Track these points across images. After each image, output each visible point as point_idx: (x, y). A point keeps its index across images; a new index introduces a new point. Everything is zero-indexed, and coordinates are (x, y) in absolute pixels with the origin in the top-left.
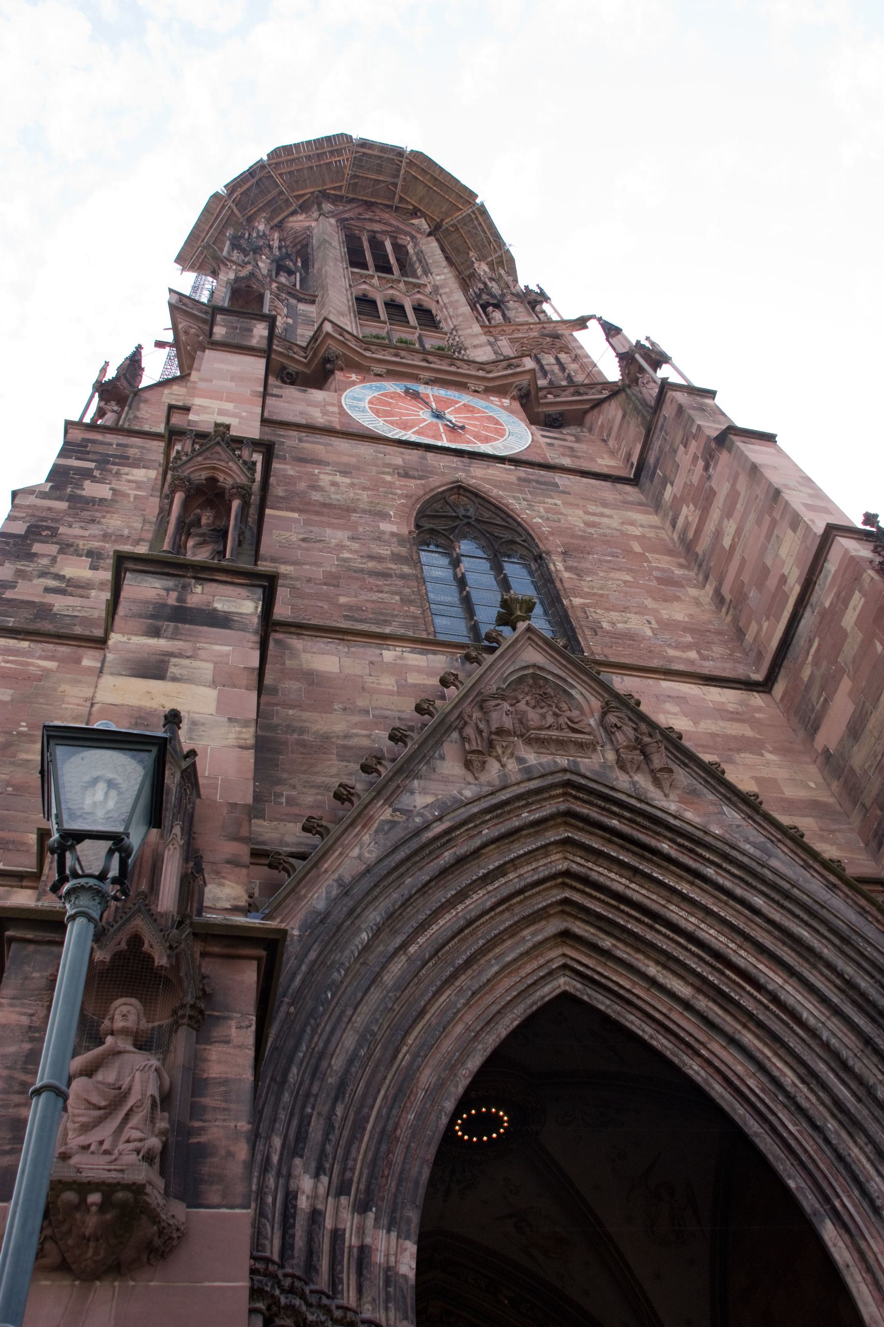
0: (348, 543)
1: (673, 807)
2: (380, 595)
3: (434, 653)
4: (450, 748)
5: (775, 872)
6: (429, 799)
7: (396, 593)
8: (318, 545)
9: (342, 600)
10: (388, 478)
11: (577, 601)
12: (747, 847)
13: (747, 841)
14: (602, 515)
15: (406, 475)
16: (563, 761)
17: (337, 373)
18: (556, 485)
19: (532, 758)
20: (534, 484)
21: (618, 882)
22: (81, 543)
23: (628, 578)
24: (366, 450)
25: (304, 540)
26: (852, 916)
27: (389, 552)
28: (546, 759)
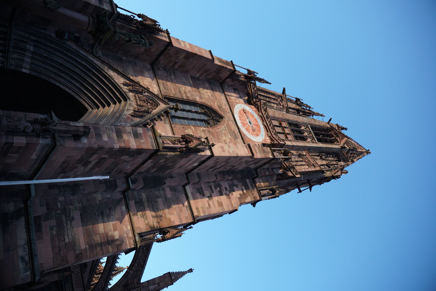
15: (219, 106)
18: (237, 138)
20: (234, 134)
24: (225, 102)
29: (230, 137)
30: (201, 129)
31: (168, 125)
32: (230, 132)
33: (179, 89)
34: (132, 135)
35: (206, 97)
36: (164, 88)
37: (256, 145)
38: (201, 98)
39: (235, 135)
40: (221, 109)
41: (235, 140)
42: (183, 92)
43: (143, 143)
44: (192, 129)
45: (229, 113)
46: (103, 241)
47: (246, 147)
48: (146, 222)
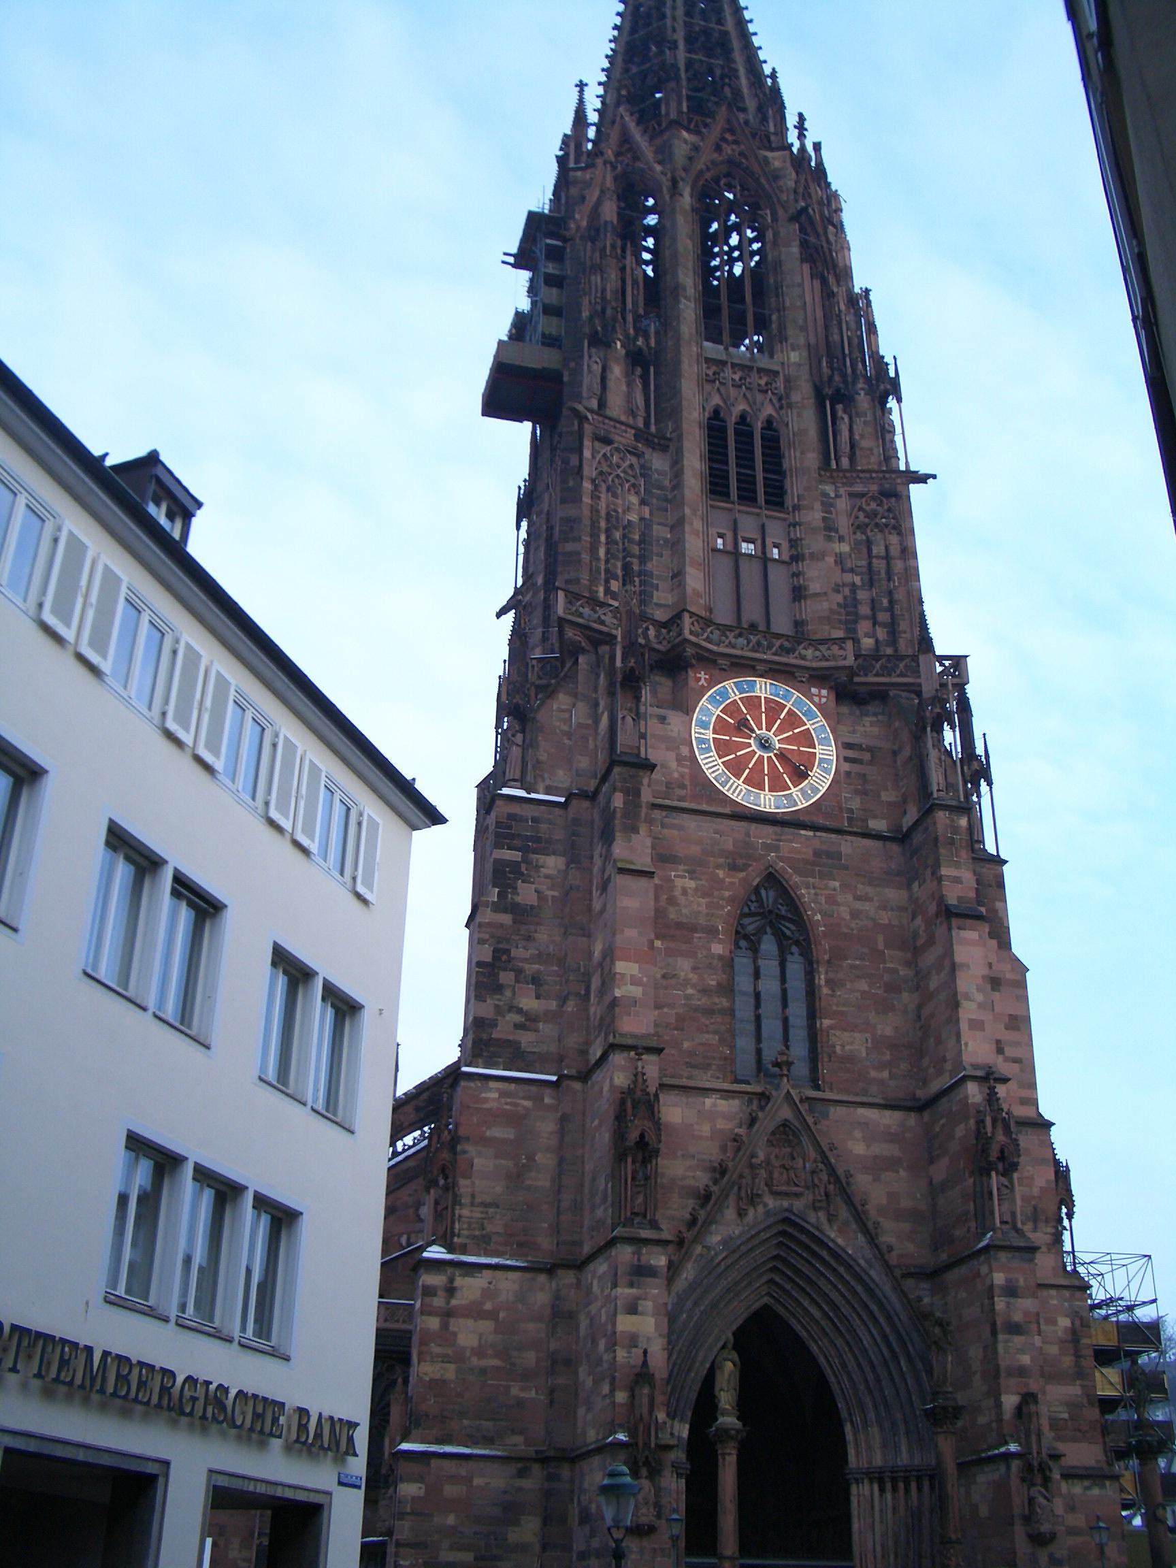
0: (691, 975)
1: (833, 1235)
2: (707, 1036)
3: (733, 1098)
4: (732, 1200)
5: (872, 1279)
6: (719, 1238)
7: (716, 1032)
8: (673, 981)
9: (686, 1045)
10: (721, 873)
11: (826, 1022)
12: (862, 1262)
13: (863, 1257)
14: (867, 898)
15: (734, 868)
16: (786, 1204)
17: (690, 673)
18: (837, 856)
19: (771, 1202)
21: (800, 1265)
22: (527, 966)
23: (866, 988)
25: (664, 976)
26: (898, 1306)
27: (714, 983)
28: (778, 1203)
29: (837, 884)
30: (825, 990)
31: (832, 1109)
32: (822, 876)
33: (696, 1009)
34: (1012, 1300)
35: (703, 909)
36: (706, 1067)
37: (848, 774)
38: (712, 932)
39: (829, 855)
40: (740, 862)
41: (846, 868)
42: (704, 1001)
43: (1025, 1281)
44: (831, 1027)
45: (748, 835)
46: (1072, 1352)
47: (959, 928)
48: (1044, 1249)
